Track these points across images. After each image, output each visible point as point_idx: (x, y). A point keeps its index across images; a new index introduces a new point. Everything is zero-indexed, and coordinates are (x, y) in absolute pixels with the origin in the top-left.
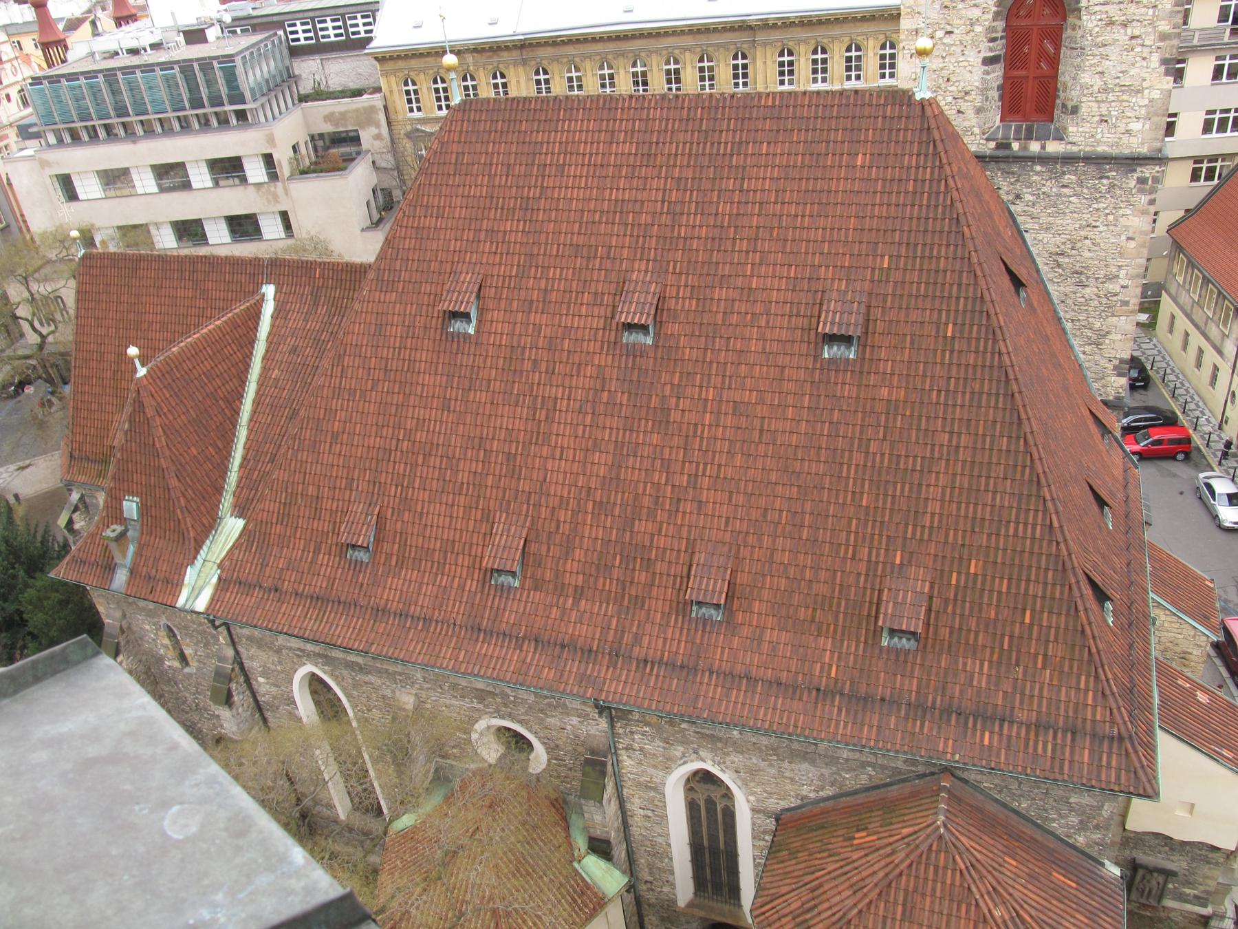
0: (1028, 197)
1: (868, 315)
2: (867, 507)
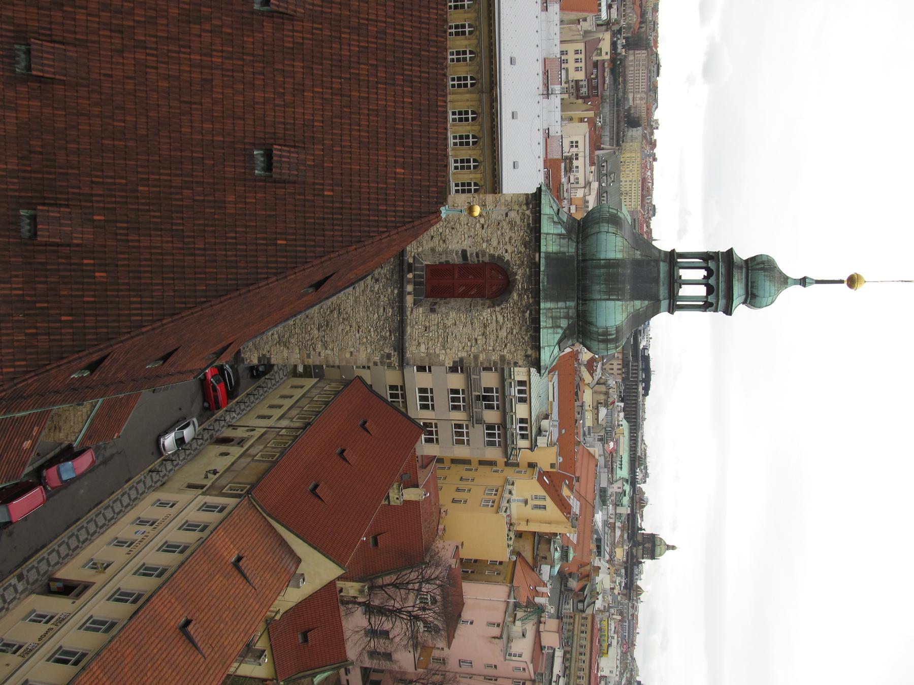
1: (289, 182)
2: (137, 191)
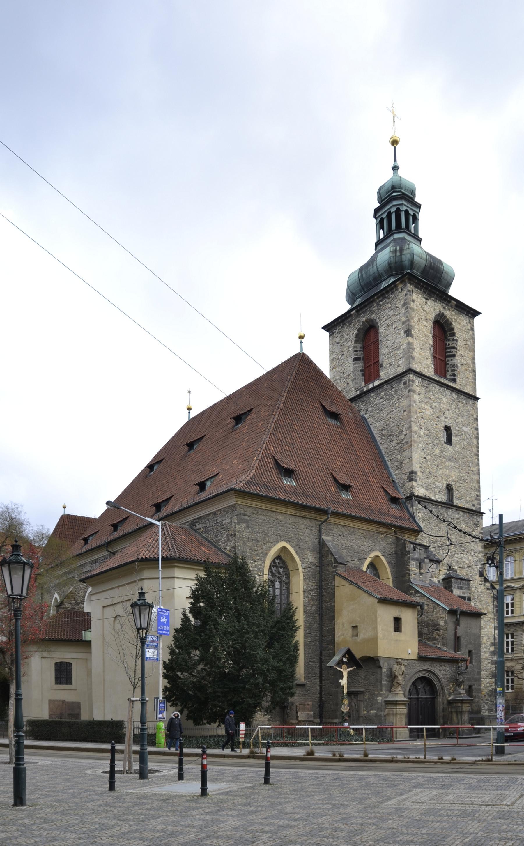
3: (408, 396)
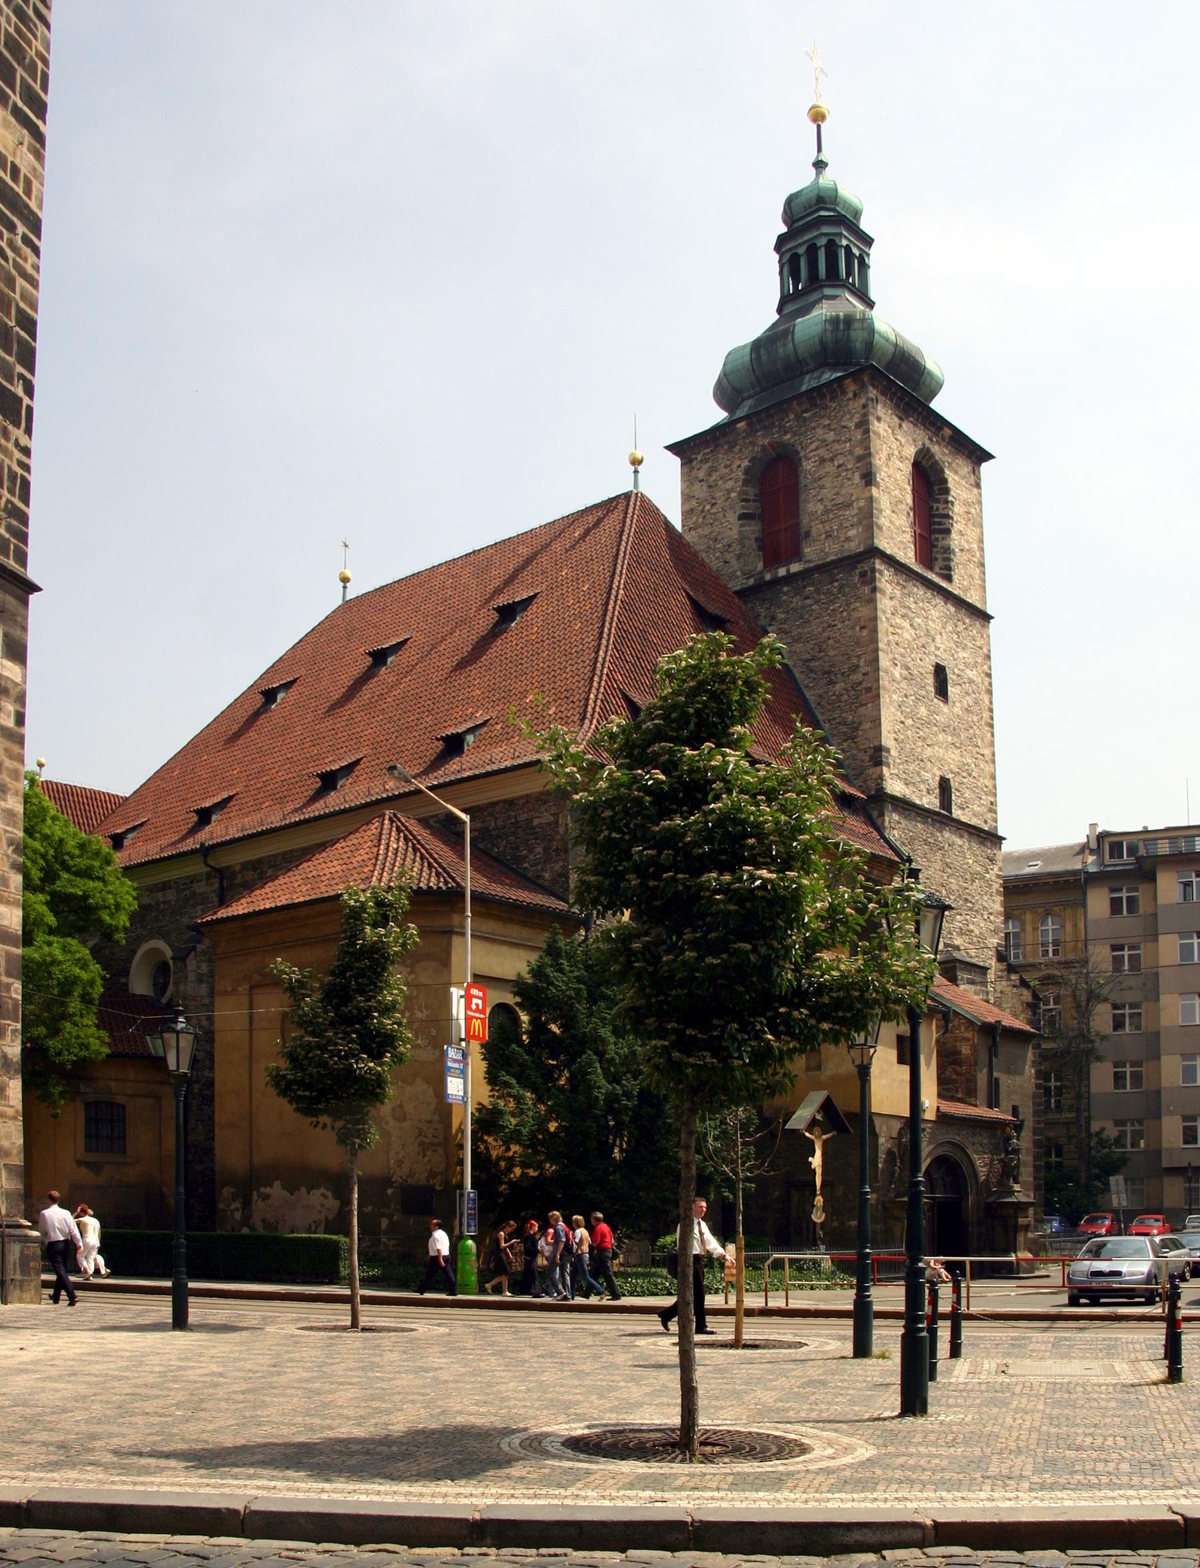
0: (781, 616)
3: (872, 601)
